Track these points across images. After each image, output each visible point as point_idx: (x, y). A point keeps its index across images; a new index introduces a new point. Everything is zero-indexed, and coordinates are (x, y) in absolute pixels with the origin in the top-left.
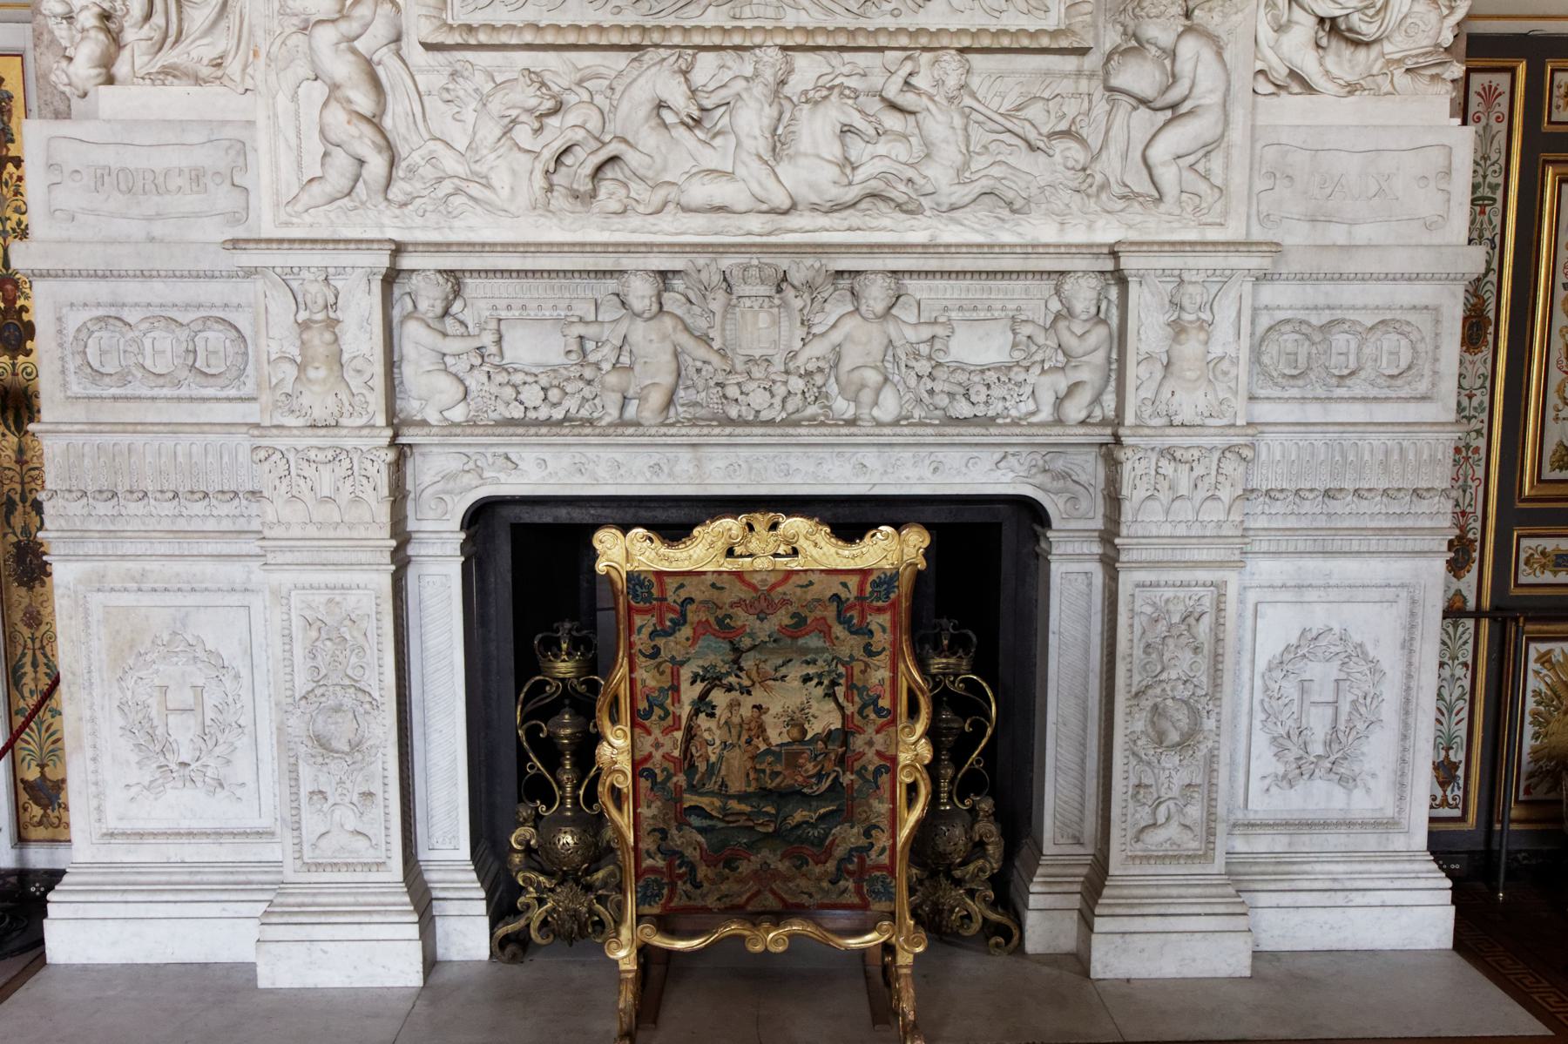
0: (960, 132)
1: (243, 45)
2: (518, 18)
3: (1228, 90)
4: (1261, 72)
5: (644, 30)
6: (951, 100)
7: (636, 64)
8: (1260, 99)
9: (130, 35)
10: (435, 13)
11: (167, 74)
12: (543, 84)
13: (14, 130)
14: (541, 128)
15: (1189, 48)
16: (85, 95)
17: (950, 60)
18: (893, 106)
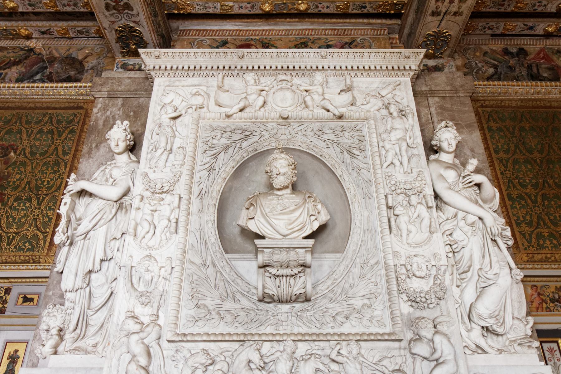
0: (359, 370)
1: (105, 340)
2: (201, 331)
3: (455, 351)
4: (466, 346)
5: (245, 335)
6: (355, 358)
7: (242, 347)
8: (468, 356)
9: (67, 336)
10: (173, 330)
11: (76, 350)
12: (208, 354)
13: (16, 370)
14: (206, 370)
15: (438, 339)
16: (45, 358)
17: (353, 345)
18: (334, 361)
